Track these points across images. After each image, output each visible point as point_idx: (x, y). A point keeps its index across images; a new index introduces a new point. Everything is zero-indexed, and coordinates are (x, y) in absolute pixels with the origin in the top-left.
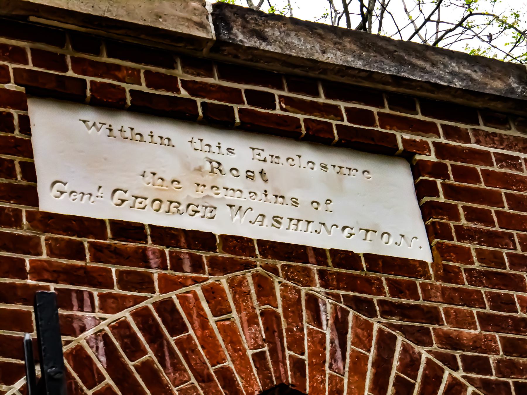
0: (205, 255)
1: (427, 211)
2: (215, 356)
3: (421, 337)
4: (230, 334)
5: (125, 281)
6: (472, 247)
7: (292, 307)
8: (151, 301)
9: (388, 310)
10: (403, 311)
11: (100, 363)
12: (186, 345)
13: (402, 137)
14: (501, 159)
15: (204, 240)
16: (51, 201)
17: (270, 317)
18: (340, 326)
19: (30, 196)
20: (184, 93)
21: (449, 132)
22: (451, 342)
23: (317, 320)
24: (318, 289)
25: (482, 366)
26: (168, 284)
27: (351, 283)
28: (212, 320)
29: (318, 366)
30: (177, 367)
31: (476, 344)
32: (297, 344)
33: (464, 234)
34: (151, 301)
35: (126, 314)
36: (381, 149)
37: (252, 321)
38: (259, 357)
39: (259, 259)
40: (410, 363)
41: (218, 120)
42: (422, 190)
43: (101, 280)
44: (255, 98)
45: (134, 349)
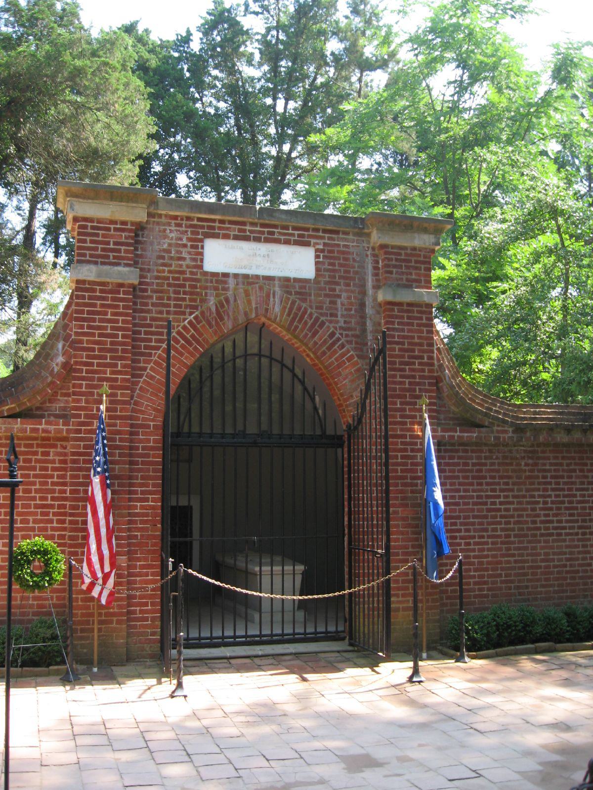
0: (246, 281)
1: (317, 263)
3: (304, 300)
11: (213, 309)
13: (313, 241)
14: (345, 246)
15: (246, 276)
19: (201, 267)
20: (248, 233)
21: (329, 238)
23: (274, 297)
24: (277, 289)
25: (321, 308)
31: (320, 302)
40: (299, 308)
41: (257, 240)
42: (317, 257)
44: (270, 233)
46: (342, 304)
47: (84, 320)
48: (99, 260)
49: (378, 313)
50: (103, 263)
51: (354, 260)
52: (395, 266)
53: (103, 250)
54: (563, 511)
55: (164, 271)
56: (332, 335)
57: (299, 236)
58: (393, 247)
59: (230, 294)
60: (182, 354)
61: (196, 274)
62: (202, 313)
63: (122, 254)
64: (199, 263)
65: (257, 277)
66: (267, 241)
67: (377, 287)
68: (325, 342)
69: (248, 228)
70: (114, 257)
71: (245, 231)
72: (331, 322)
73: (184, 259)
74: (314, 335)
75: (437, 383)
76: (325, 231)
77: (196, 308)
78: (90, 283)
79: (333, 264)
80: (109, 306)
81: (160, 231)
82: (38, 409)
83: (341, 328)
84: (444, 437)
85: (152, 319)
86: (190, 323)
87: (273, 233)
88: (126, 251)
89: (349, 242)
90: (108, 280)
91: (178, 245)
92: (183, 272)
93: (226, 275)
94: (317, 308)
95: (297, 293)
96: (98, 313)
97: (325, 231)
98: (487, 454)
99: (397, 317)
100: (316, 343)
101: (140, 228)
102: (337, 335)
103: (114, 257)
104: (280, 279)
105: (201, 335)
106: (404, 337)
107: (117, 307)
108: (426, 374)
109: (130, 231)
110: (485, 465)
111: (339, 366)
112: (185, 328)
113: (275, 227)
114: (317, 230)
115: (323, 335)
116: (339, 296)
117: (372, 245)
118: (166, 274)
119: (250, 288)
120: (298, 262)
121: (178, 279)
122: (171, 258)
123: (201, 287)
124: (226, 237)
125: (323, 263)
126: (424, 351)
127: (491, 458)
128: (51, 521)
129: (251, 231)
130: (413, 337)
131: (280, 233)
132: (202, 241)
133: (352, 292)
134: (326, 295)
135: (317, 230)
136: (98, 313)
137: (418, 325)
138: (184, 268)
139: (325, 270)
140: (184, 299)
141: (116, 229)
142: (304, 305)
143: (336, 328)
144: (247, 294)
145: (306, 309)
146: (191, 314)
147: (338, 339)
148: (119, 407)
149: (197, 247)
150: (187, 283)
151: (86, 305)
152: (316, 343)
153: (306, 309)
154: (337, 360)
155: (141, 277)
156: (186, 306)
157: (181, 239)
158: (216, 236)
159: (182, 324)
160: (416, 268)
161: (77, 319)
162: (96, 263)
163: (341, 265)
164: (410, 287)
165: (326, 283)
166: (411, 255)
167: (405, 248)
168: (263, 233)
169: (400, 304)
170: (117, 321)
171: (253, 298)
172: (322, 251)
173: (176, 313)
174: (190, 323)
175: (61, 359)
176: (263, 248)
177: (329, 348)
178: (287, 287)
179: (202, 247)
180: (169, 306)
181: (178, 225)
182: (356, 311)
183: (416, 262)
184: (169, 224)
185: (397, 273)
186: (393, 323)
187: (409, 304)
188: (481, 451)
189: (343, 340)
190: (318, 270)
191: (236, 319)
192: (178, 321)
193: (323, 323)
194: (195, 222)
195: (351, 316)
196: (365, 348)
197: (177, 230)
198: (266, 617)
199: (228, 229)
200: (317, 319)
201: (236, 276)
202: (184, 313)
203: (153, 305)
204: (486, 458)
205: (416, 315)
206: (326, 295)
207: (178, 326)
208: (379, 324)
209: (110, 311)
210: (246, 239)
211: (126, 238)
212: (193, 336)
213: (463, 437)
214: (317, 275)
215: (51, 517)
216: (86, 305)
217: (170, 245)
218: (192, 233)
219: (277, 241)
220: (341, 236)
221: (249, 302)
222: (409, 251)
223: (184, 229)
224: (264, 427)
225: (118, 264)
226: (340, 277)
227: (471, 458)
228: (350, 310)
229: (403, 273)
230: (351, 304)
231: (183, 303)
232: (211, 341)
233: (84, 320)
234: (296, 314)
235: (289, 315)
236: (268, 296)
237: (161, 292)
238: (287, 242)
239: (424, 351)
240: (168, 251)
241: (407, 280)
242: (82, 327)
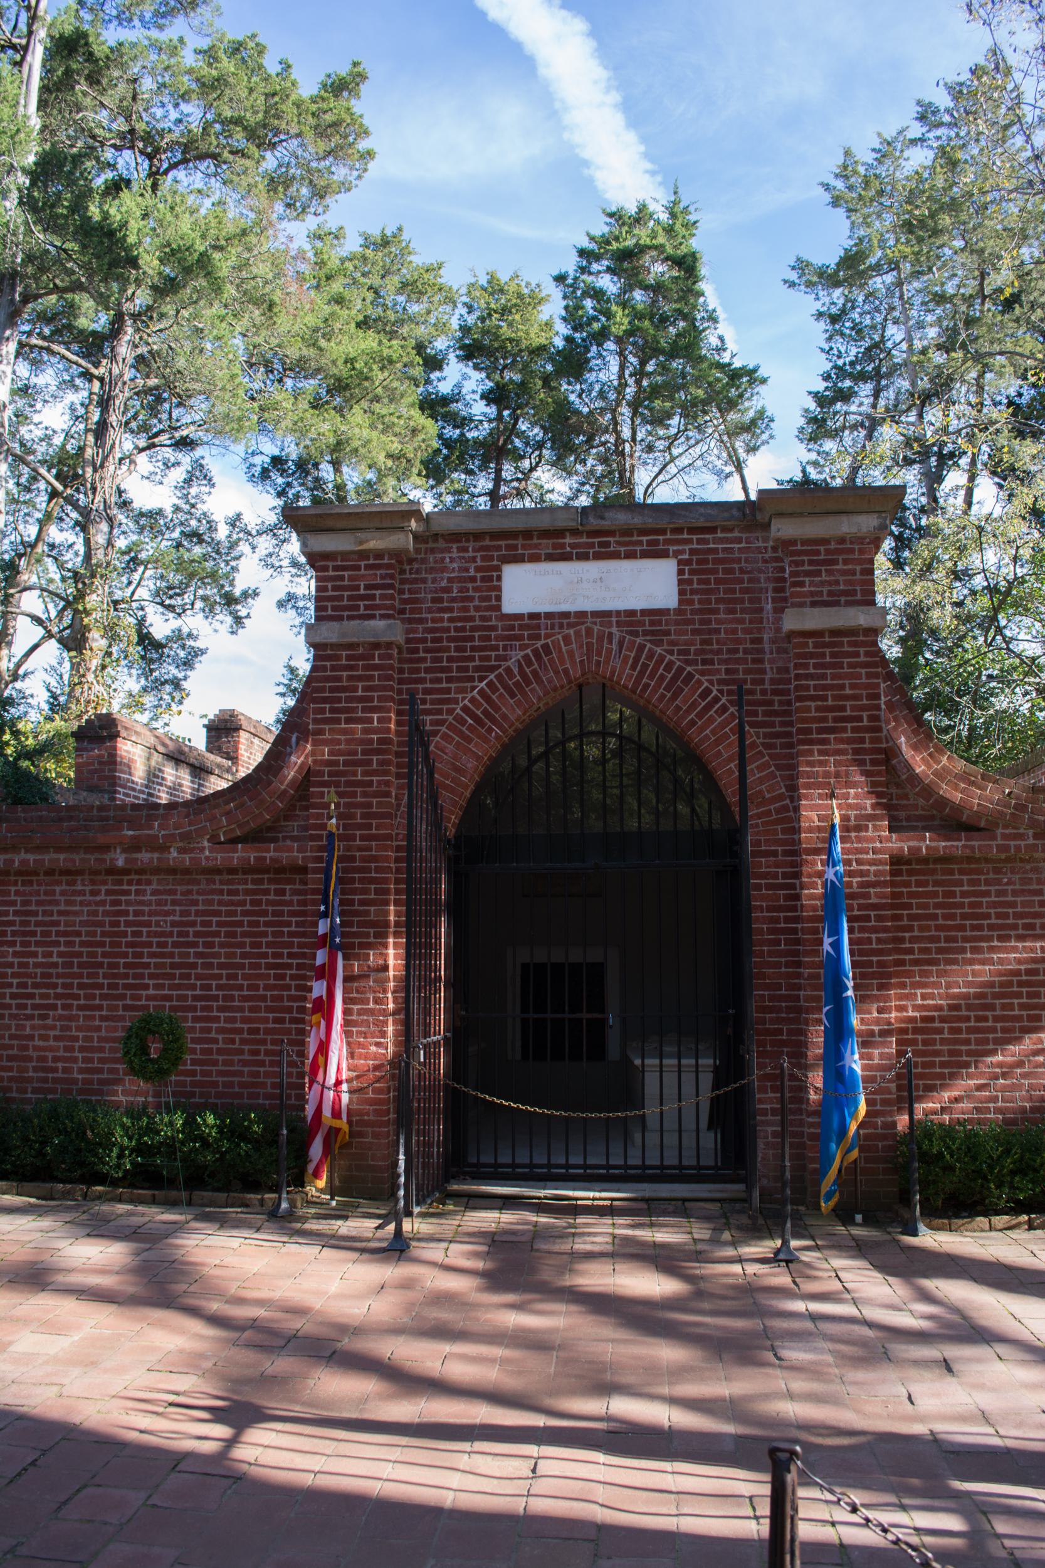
1: (680, 582)
2: (562, 663)
3: (658, 643)
4: (571, 654)
5: (530, 637)
6: (696, 597)
7: (600, 639)
8: (539, 644)
9: (645, 633)
10: (652, 633)
12: (551, 661)
13: (672, 548)
14: (724, 549)
15: (566, 615)
17: (589, 645)
18: (621, 644)
21: (699, 541)
22: (672, 643)
23: (610, 643)
24: (614, 630)
25: (686, 652)
26: (547, 636)
27: (631, 624)
28: (564, 649)
29: (607, 662)
30: (546, 669)
31: (687, 643)
32: (599, 654)
33: (693, 592)
34: (539, 644)
35: (529, 651)
36: (662, 555)
37: (581, 647)
38: (582, 662)
39: (590, 620)
41: (583, 557)
42: (680, 572)
43: (519, 638)
45: (529, 663)
47: (325, 700)
48: (346, 614)
50: (350, 618)
52: (808, 574)
53: (350, 598)
54: (49, 1022)
55: (442, 620)
56: (707, 692)
57: (649, 543)
58: (805, 542)
60: (470, 740)
61: (489, 619)
63: (378, 602)
64: (494, 603)
65: (582, 614)
66: (598, 557)
68: (694, 705)
69: (568, 540)
70: (367, 607)
71: (563, 546)
72: (703, 673)
73: (471, 599)
74: (675, 697)
75: (887, 761)
76: (692, 530)
77: (492, 669)
78: (333, 646)
79: (707, 582)
80: (360, 678)
81: (435, 562)
82: (270, 829)
83: (720, 682)
84: (902, 848)
86: (482, 692)
87: (607, 544)
88: (383, 597)
90: (355, 640)
91: (460, 580)
92: (471, 619)
93: (534, 616)
94: (680, 652)
95: (645, 633)
97: (692, 530)
98: (991, 876)
99: (812, 655)
100: (678, 708)
102: (715, 692)
103: (367, 607)
105: (497, 709)
106: (825, 688)
107: (370, 678)
108: (867, 746)
109: (388, 566)
110: (987, 894)
111: (718, 742)
112: (473, 700)
113: (610, 533)
114: (679, 530)
117: (771, 543)
118: (446, 624)
119: (572, 631)
121: (463, 629)
123: (496, 639)
124: (535, 559)
125: (690, 582)
126: (862, 708)
127: (998, 882)
128: (288, 988)
129: (572, 546)
130: (842, 687)
131: (618, 543)
132: (498, 569)
133: (741, 621)
134: (695, 632)
135: (679, 530)
137: (851, 665)
138: (472, 613)
139: (693, 592)
140: (472, 659)
141: (367, 567)
142: (659, 650)
143: (711, 682)
145: (662, 658)
146: (481, 679)
147: (716, 700)
148: (374, 822)
149: (490, 579)
150: (477, 634)
151: (327, 679)
152: (678, 708)
153: (662, 658)
154: (713, 732)
155: (408, 631)
156: (477, 669)
157: (467, 570)
158: (518, 559)
159: (469, 696)
161: (315, 701)
162: (341, 618)
163: (718, 581)
164: (836, 604)
167: (825, 541)
168: (592, 545)
170: (371, 699)
172: (688, 562)
173: (459, 679)
174: (482, 692)
176: (591, 569)
177: (700, 716)
178: (631, 624)
179: (499, 578)
180: (448, 670)
181: (460, 550)
182: (745, 651)
184: (449, 550)
185: (811, 584)
186: (805, 666)
187: (835, 632)
188: (979, 872)
189: (724, 700)
190: (681, 592)
192: (462, 690)
193: (690, 676)
195: (738, 661)
197: (461, 558)
198: (653, 1139)
199: (536, 546)
200: (680, 670)
201: (549, 615)
202: (471, 679)
203: (427, 670)
204: (988, 882)
206: (695, 632)
207: (463, 699)
208: (787, 670)
209: (360, 684)
210: (565, 557)
211: (382, 578)
212: (485, 712)
213: (937, 849)
214: (681, 602)
215: (288, 981)
216: (327, 679)
217: (450, 580)
218: (483, 558)
219: (615, 556)
222: (833, 546)
223: (471, 554)
225: (373, 617)
226: (718, 601)
227: (960, 883)
228: (736, 651)
229: (822, 583)
231: (471, 664)
233: (325, 700)
234: (645, 666)
235: (633, 668)
237: (439, 650)
238: (631, 555)
239: (862, 708)
240: (447, 590)
242: (323, 711)
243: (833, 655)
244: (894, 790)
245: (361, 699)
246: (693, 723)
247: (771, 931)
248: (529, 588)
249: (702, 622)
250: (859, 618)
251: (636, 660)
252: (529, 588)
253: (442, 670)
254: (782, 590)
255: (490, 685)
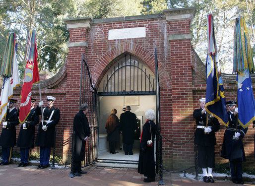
3: (141, 45)
16: (109, 39)
18: (133, 45)
42: (146, 29)
44: (129, 25)
46: (155, 44)
47: (71, 59)
49: (169, 45)
51: (160, 29)
56: (152, 55)
59: (116, 46)
62: (107, 53)
67: (168, 37)
68: (149, 58)
77: (105, 52)
85: (92, 57)
87: (131, 24)
89: (158, 22)
93: (114, 40)
94: (146, 46)
95: (139, 43)
96: (75, 56)
101: (88, 30)
104: (133, 39)
106: (178, 53)
115: (148, 55)
116: (154, 42)
120: (140, 32)
121: (100, 43)
122: (98, 37)
124: (115, 28)
130: (182, 52)
136: (75, 56)
137: (184, 48)
144: (122, 45)
151: (72, 54)
160: (183, 27)
165: (149, 38)
166: (181, 23)
169: (176, 41)
171: (123, 46)
175: (64, 71)
183: (183, 25)
187: (180, 40)
190: (146, 34)
191: (118, 54)
194: (106, 25)
196: (164, 59)
200: (146, 50)
205: (183, 44)
220: (155, 21)
221: (122, 47)
222: (180, 22)
224: (132, 89)
226: (154, 35)
230: (159, 44)
232: (110, 62)
233: (71, 59)
236: (129, 45)
241: (179, 32)
243: (179, 45)
244: (194, 75)
245: (78, 58)
246: (148, 62)
247: (165, 107)
248: (114, 34)
249: (151, 40)
250: (187, 37)
251: (136, 49)
252: (114, 34)
253: (96, 52)
254: (169, 32)
255: (105, 55)
